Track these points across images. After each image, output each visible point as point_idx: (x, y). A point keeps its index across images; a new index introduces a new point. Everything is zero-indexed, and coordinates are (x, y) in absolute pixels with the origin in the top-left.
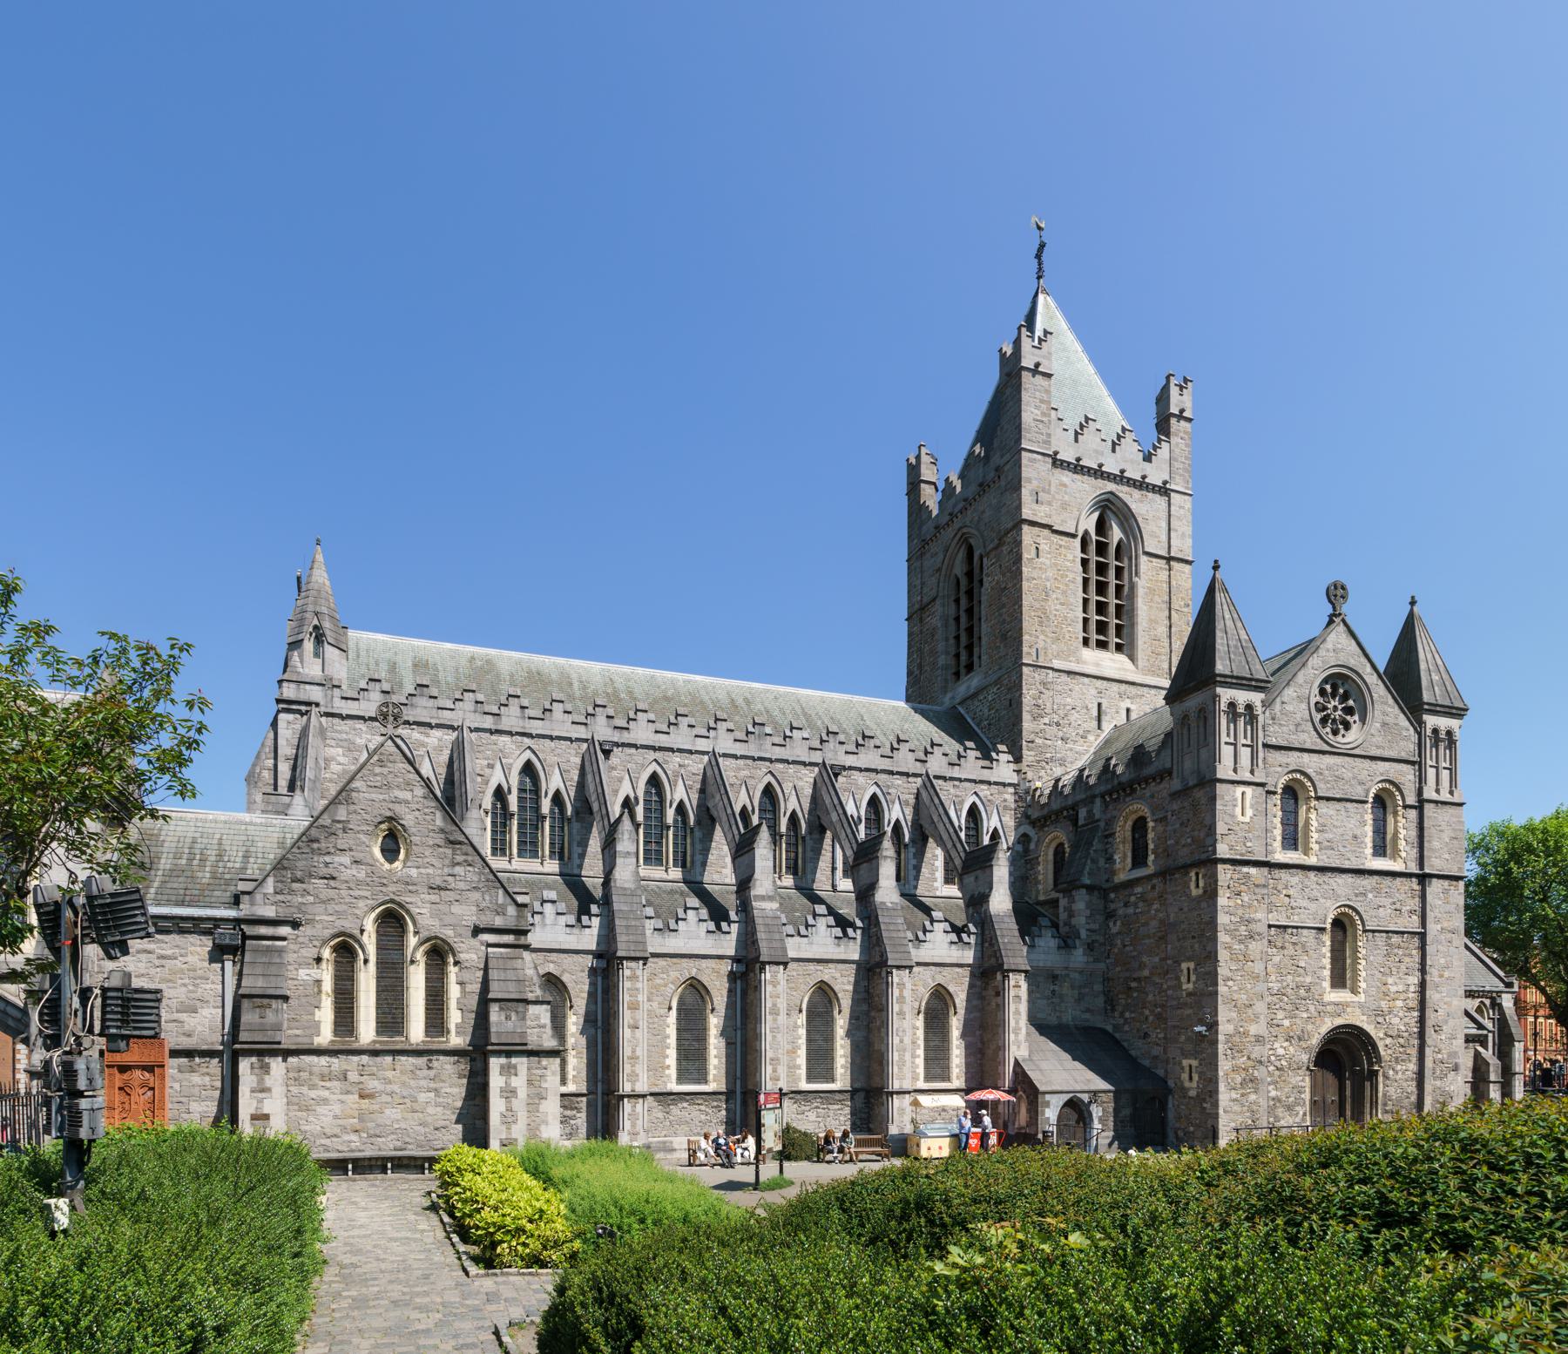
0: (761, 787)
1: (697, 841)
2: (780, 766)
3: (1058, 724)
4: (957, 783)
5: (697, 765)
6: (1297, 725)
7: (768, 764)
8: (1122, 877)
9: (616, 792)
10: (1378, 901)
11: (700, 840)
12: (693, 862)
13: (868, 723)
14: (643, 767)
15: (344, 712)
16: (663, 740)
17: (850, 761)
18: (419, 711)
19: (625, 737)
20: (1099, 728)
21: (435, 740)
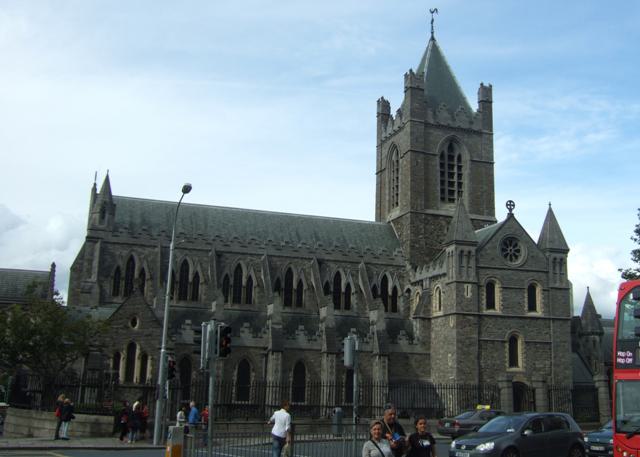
8: (435, 315)
16: (245, 250)
17: (327, 257)
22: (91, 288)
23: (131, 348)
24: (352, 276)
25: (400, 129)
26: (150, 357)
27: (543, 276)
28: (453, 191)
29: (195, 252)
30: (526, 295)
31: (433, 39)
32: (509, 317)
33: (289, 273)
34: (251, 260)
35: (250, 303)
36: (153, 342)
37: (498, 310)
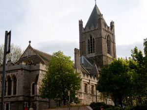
25: (95, 30)
31: (96, 5)
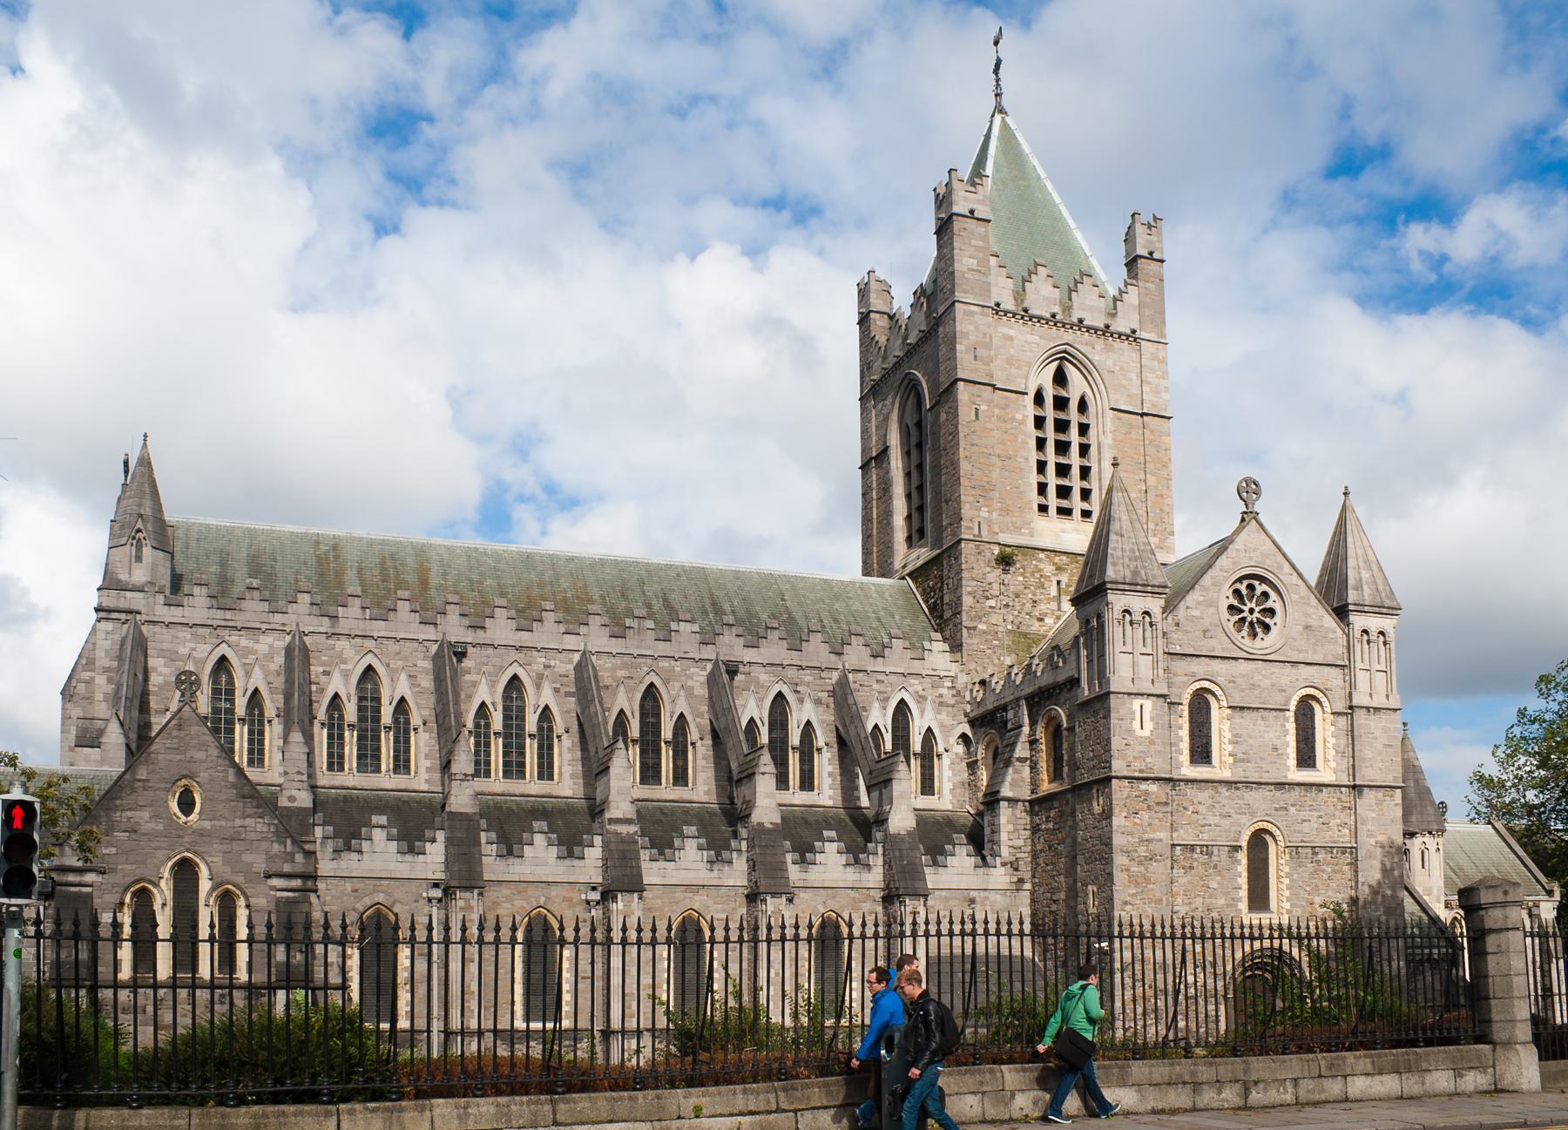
0: (643, 687)
1: (565, 750)
2: (665, 664)
3: (1007, 606)
4: (881, 677)
5: (566, 666)
6: (1205, 632)
7: (649, 661)
9: (470, 697)
10: (1304, 814)
11: (569, 750)
12: (560, 774)
13: (789, 603)
14: (502, 669)
15: (167, 621)
16: (525, 638)
17: (749, 655)
18: (248, 615)
19: (480, 636)
20: (1059, 609)
21: (266, 646)
22: (101, 732)
23: (185, 873)
24: (818, 702)
26: (241, 902)
27: (1334, 678)
28: (1070, 489)
29: (393, 647)
30: (1291, 727)
32: (1248, 784)
33: (651, 697)
34: (546, 667)
35: (551, 778)
36: (247, 858)
37: (1220, 769)
